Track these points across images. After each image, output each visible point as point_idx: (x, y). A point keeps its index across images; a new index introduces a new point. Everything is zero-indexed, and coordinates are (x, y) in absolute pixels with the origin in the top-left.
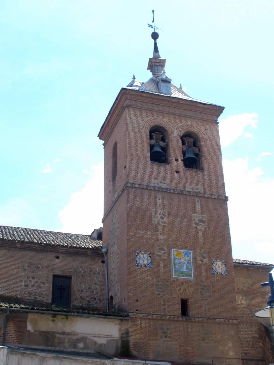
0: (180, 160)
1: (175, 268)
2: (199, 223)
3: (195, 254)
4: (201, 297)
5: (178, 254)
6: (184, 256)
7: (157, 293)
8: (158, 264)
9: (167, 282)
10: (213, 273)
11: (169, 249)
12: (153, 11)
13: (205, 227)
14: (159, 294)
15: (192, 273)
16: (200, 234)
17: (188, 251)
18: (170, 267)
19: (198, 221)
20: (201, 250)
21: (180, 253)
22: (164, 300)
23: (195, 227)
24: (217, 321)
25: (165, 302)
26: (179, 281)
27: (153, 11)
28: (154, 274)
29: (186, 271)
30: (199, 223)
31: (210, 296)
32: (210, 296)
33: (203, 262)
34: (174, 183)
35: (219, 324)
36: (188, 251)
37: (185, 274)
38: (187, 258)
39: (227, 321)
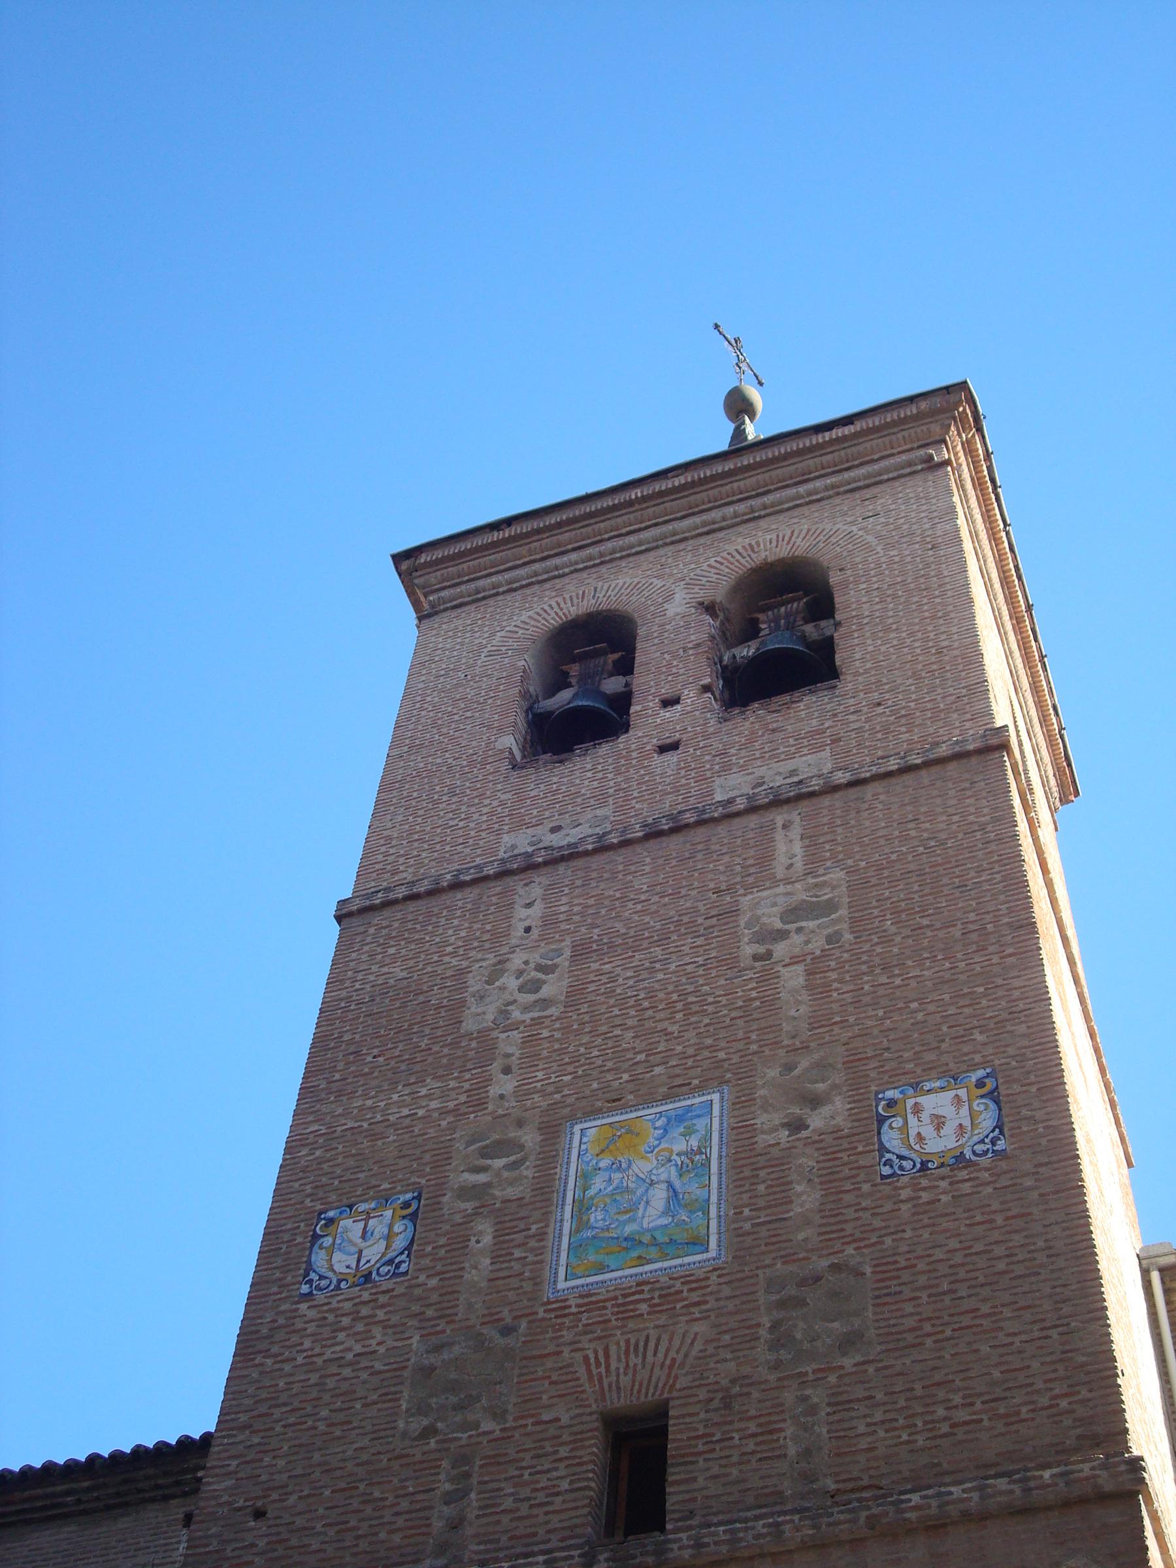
0: (690, 696)
1: (581, 1222)
2: (787, 927)
3: (742, 1103)
4: (777, 1366)
5: (613, 1139)
6: (660, 1139)
7: (417, 1424)
8: (460, 1243)
9: (507, 1331)
10: (883, 1177)
11: (552, 1131)
12: (717, 327)
13: (826, 932)
14: (428, 1432)
15: (713, 1224)
16: (793, 978)
17: (689, 1102)
18: (541, 1236)
19: (781, 918)
20: (789, 1068)
21: (630, 1132)
22: (462, 1459)
23: (756, 958)
24: (917, 1508)
25: (467, 1475)
26: (599, 1305)
27: (717, 327)
28: (415, 1308)
29: (665, 1221)
30: (787, 927)
31: (848, 1342)
32: (848, 1342)
33: (807, 1127)
34: (637, 802)
35: (936, 1526)
36: (689, 1102)
37: (654, 1242)
38: (680, 1146)
39: (1016, 1488)
